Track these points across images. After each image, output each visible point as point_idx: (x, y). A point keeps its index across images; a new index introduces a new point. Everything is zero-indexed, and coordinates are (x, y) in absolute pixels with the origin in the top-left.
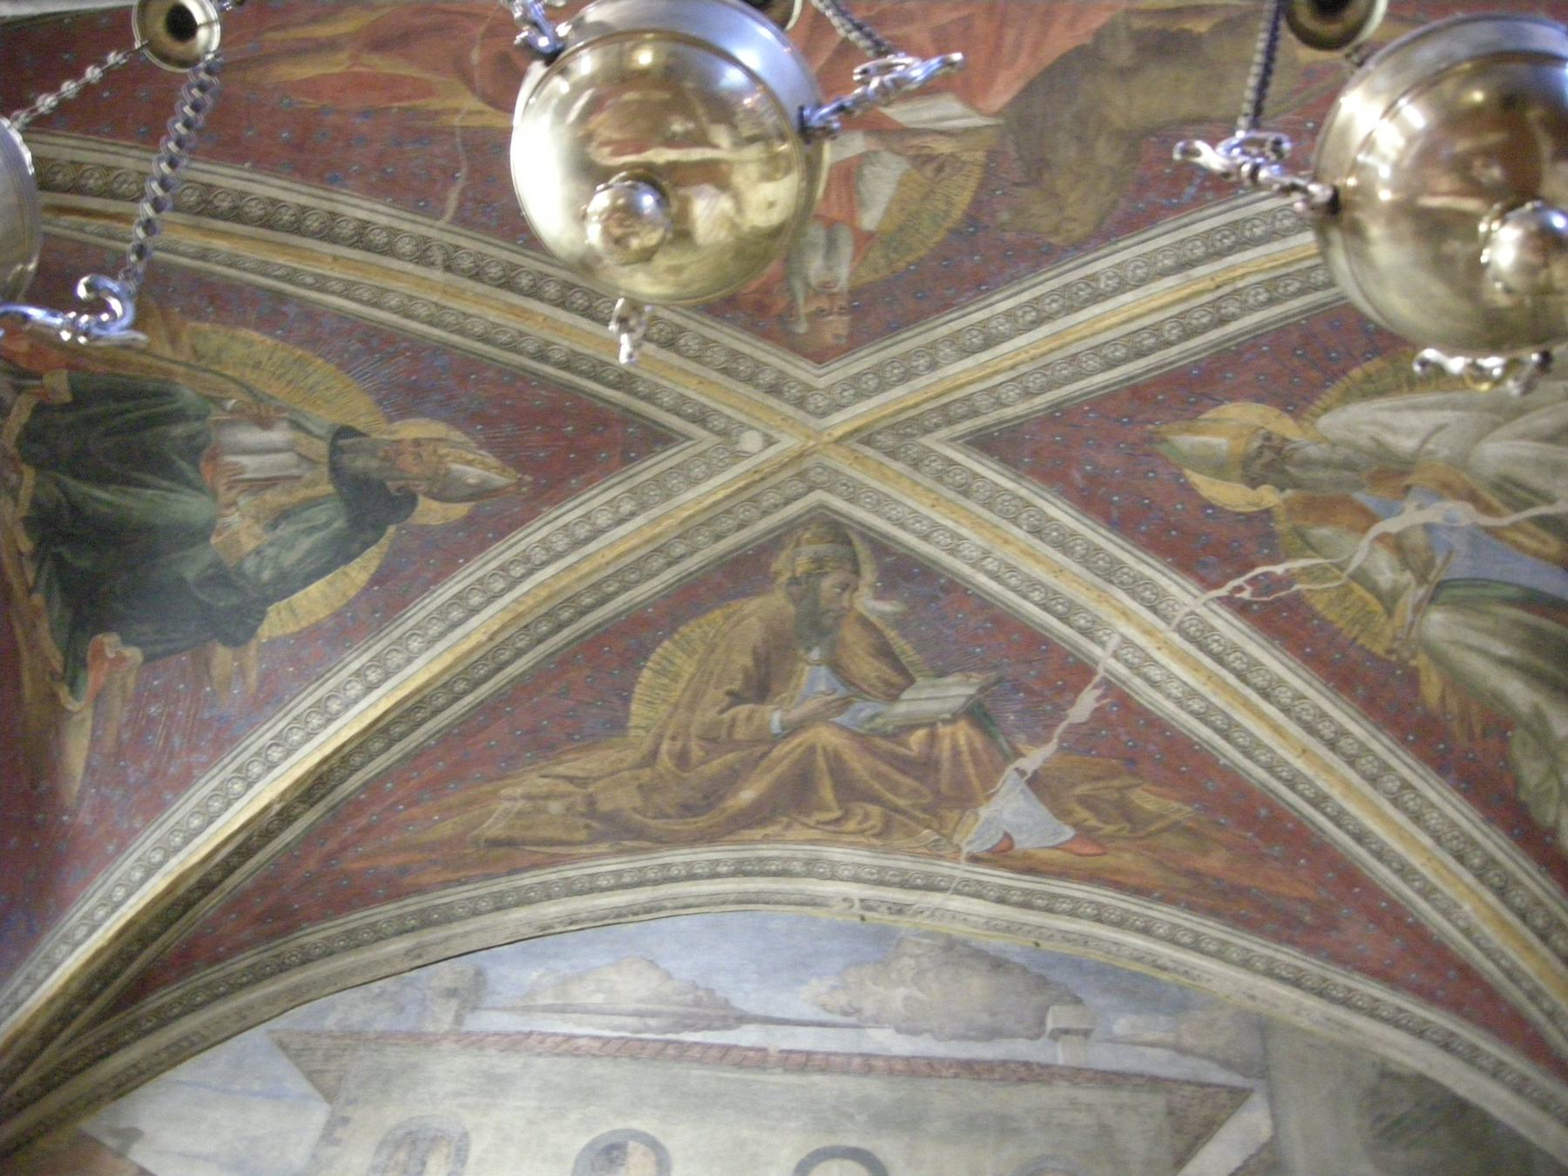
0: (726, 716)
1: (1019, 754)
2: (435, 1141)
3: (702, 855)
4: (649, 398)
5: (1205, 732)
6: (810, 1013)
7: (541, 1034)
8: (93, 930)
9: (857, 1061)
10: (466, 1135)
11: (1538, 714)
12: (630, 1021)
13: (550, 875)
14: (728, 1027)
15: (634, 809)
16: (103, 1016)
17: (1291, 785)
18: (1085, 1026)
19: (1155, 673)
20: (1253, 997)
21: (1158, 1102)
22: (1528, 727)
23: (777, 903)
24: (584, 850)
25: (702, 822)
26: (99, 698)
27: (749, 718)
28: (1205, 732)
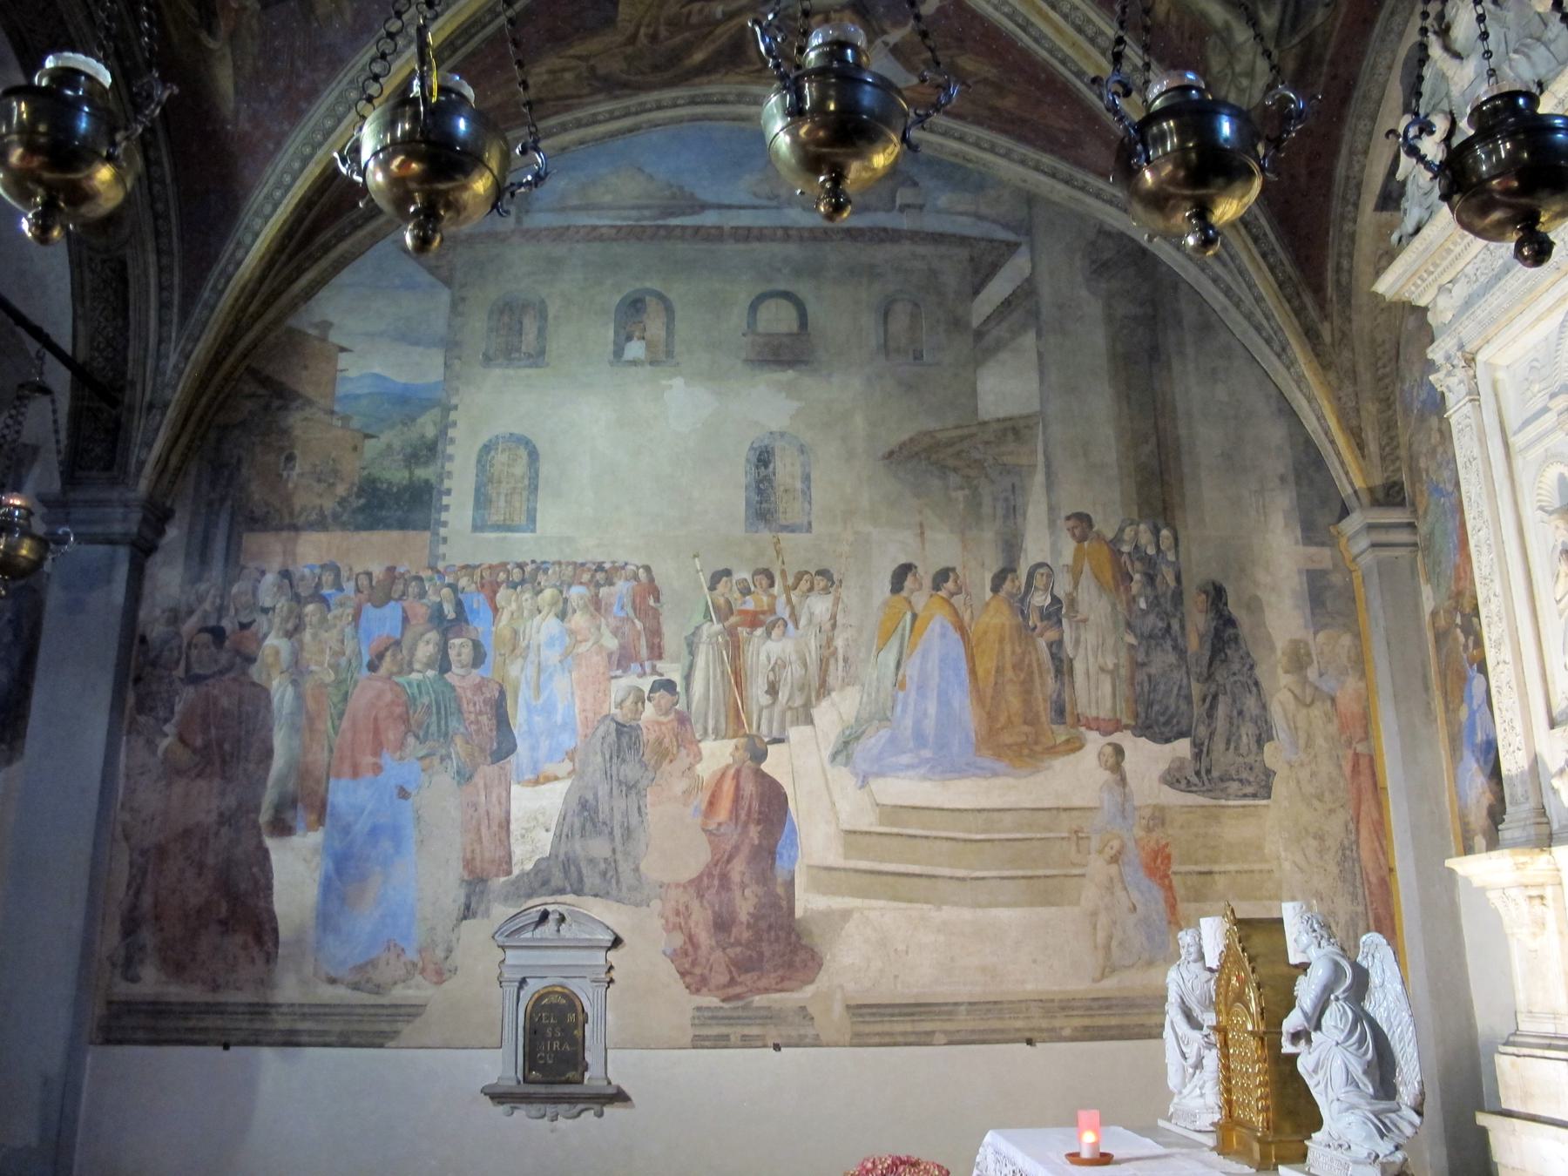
0: (685, 10)
1: (884, 32)
2: (525, 307)
3: (667, 95)
5: (1011, 26)
6: (746, 199)
7: (575, 226)
8: (275, 207)
9: (780, 233)
10: (543, 302)
11: (1228, 27)
12: (634, 213)
13: (566, 117)
14: (693, 213)
15: (622, 71)
16: (290, 258)
17: (1063, 62)
18: (920, 201)
20: (1025, 181)
21: (963, 253)
22: (1217, 32)
23: (717, 119)
24: (589, 100)
25: (667, 75)
26: (233, 36)
27: (701, 11)
28: (1011, 26)
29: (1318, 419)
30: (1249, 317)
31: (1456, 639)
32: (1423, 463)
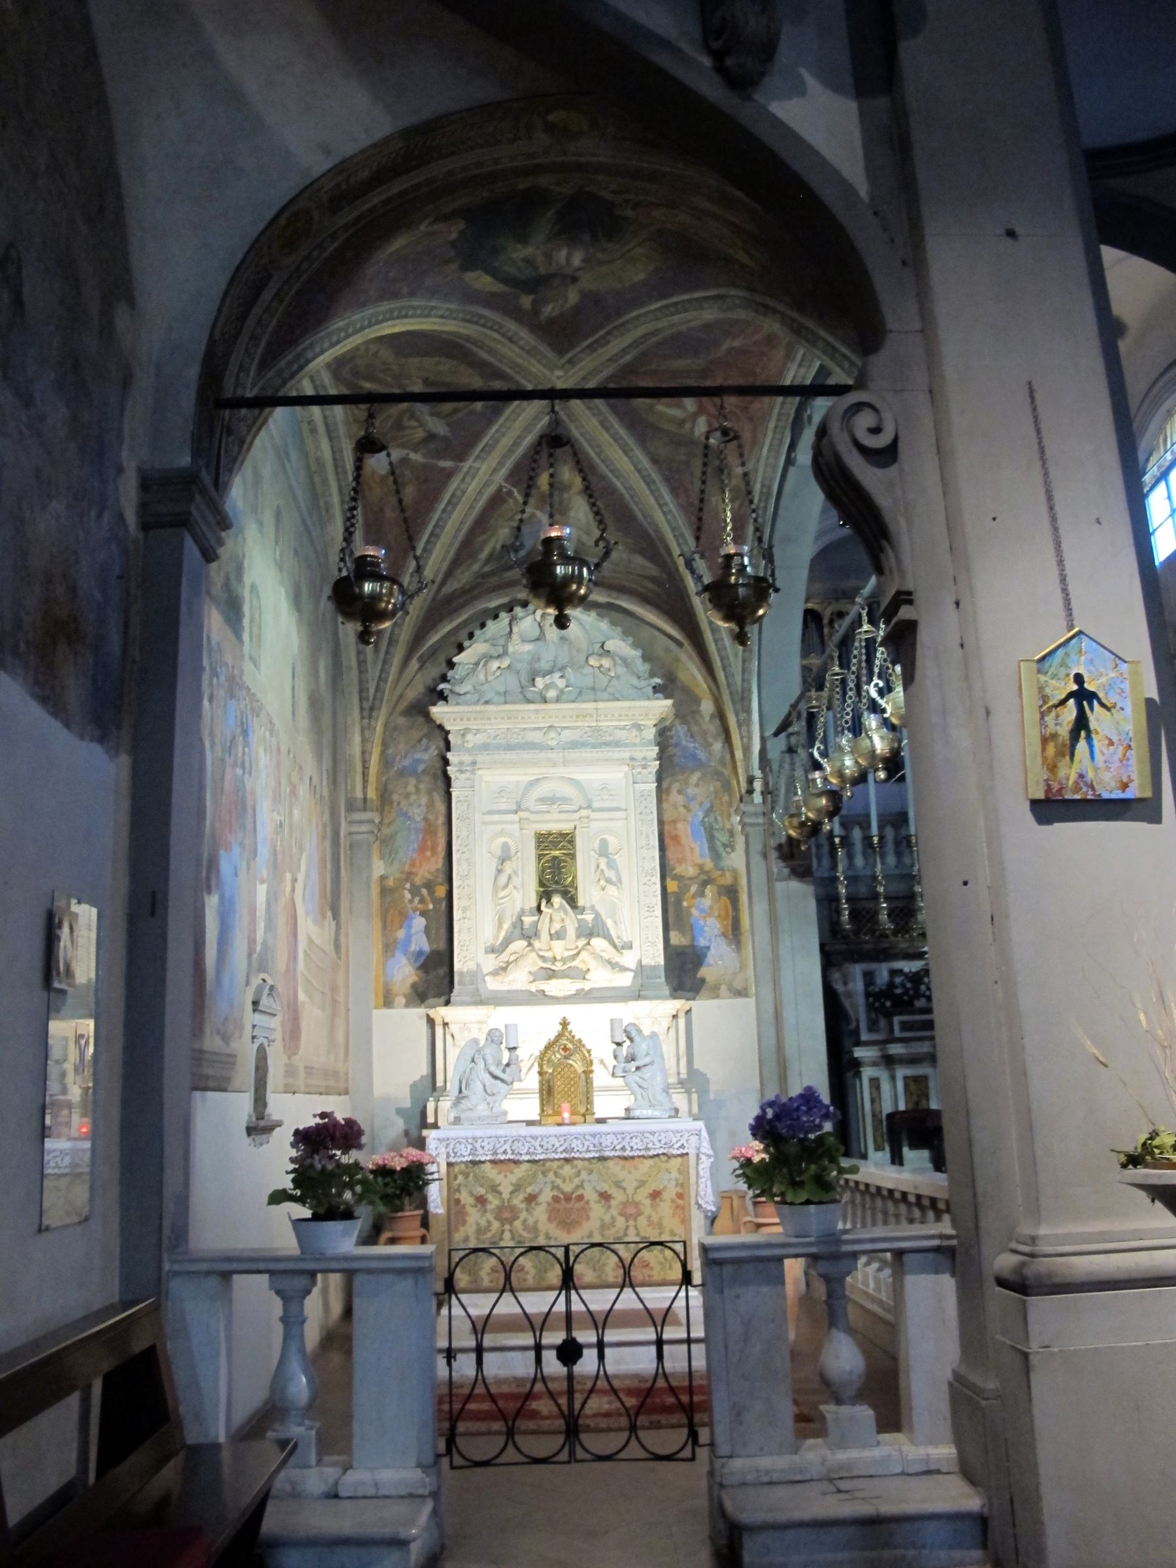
4: (582, 351)
5: (447, 497)
19: (468, 479)
28: (447, 497)
29: (363, 752)
30: (362, 683)
31: (403, 896)
32: (395, 797)
